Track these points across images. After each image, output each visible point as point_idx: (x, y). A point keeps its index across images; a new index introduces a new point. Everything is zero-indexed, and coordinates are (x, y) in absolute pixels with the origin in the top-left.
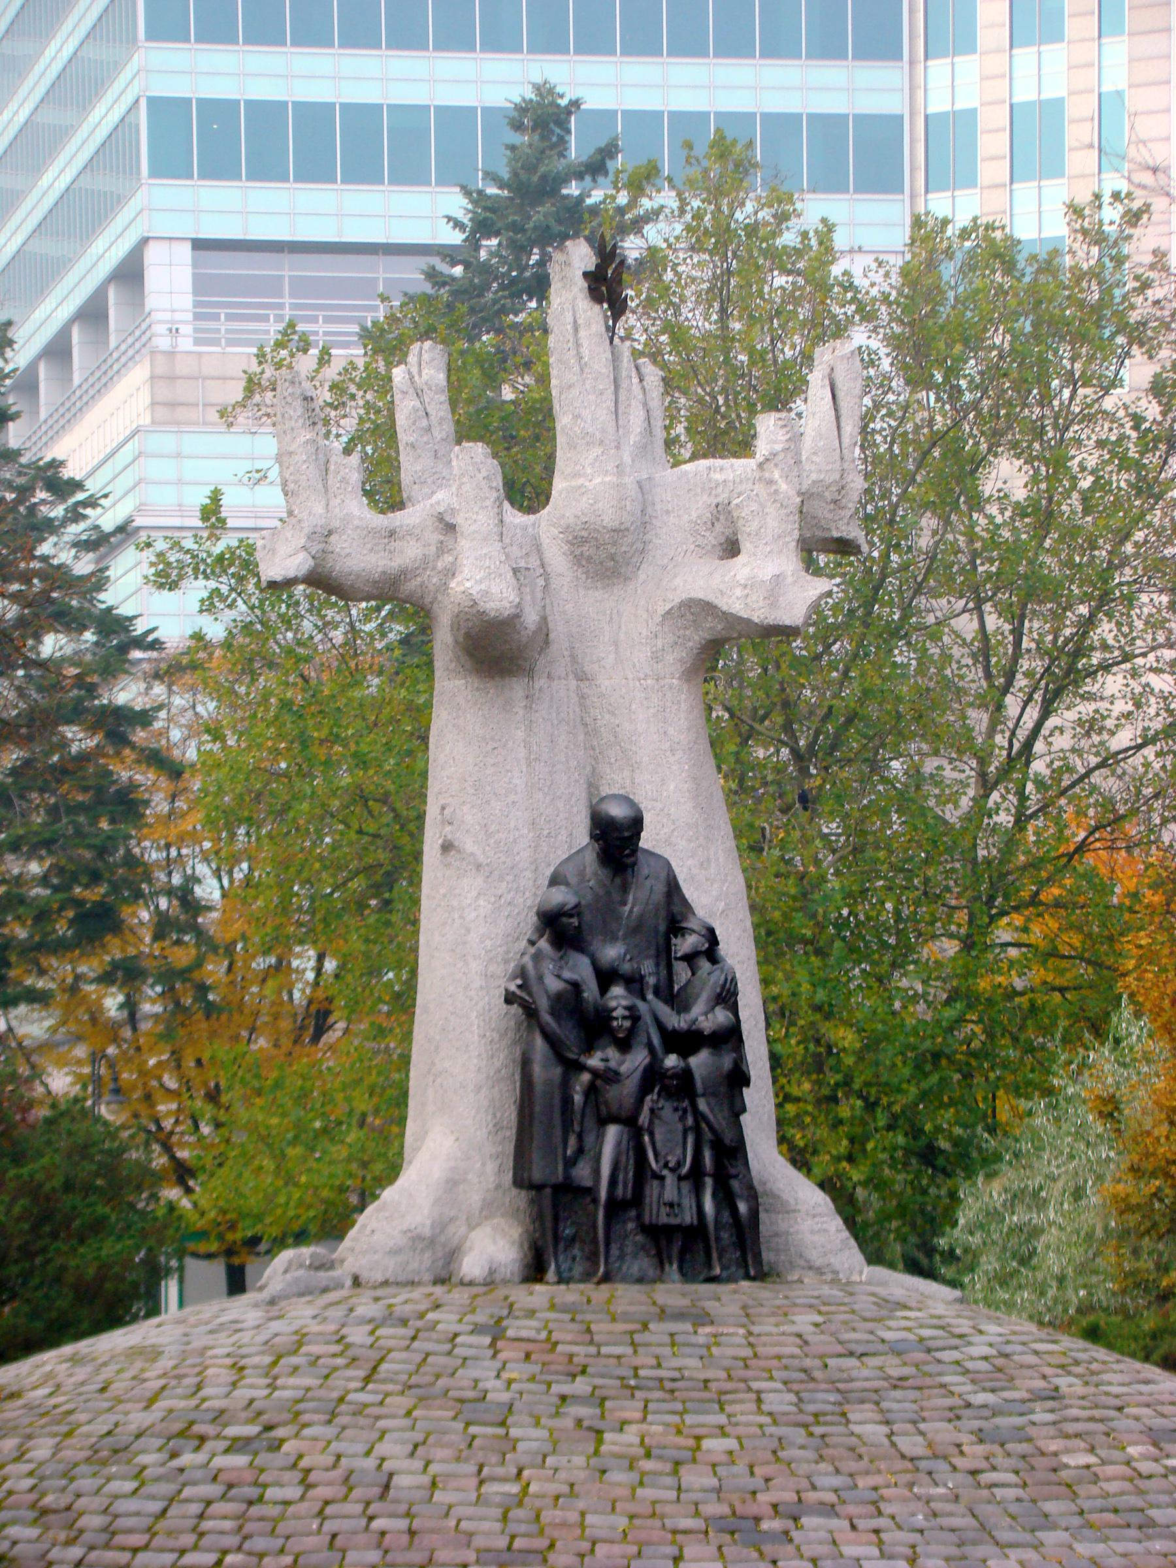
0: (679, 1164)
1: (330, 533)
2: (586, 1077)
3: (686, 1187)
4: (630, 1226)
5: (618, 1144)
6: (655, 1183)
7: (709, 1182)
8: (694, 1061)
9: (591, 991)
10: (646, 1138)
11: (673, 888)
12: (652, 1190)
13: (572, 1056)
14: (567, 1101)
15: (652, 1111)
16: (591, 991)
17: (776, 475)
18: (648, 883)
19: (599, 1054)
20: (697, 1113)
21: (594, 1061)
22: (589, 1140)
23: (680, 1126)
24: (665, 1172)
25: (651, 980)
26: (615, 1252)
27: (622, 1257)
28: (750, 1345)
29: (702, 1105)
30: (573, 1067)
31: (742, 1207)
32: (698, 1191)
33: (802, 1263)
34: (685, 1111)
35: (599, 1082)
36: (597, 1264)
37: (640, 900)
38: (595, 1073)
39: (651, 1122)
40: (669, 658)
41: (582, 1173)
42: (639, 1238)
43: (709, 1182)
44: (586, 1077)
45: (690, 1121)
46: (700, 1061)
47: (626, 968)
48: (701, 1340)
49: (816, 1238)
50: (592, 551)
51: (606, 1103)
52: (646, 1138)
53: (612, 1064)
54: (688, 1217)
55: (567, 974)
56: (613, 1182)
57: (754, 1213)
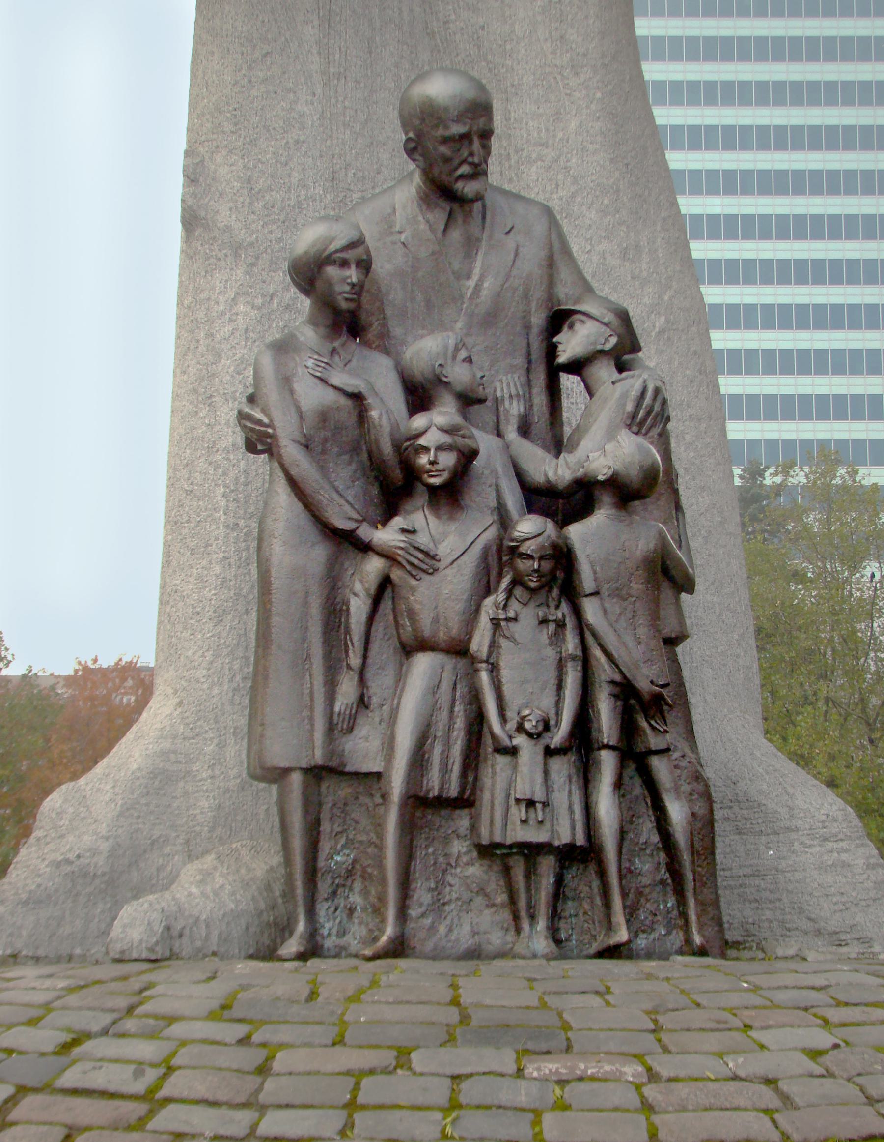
2: (374, 566)
3: (561, 768)
4: (458, 847)
5: (434, 689)
6: (502, 761)
7: (607, 762)
8: (576, 531)
9: (388, 406)
10: (484, 676)
11: (556, 255)
12: (496, 774)
13: (341, 524)
14: (334, 614)
15: (496, 623)
16: (388, 406)
18: (510, 243)
19: (398, 522)
21: (387, 536)
22: (380, 684)
23: (550, 653)
24: (520, 740)
25: (515, 409)
26: (422, 895)
27: (438, 906)
28: (647, 1107)
29: (591, 610)
30: (347, 542)
31: (677, 812)
32: (586, 775)
33: (805, 924)
34: (561, 625)
35: (396, 575)
36: (383, 921)
37: (497, 269)
38: (388, 556)
39: (493, 645)
41: (363, 749)
42: (476, 870)
43: (607, 762)
44: (374, 566)
45: (571, 644)
46: (592, 536)
47: (459, 375)
48: (522, 1094)
49: (829, 879)
51: (412, 614)
52: (484, 676)
53: (422, 540)
54: (565, 830)
55: (339, 378)
56: (419, 760)
57: (705, 827)
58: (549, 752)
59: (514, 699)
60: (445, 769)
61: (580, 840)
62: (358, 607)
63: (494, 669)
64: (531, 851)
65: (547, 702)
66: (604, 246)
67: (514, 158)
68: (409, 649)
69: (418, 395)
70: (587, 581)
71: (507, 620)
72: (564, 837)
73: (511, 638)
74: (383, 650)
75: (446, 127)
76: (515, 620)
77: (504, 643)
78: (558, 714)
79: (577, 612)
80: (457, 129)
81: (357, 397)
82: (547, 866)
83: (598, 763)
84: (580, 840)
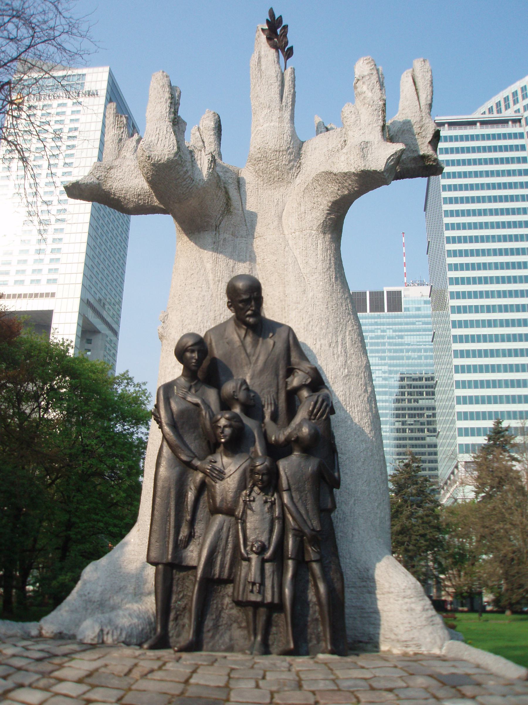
0: (263, 549)
1: (111, 168)
2: (200, 476)
6: (244, 563)
15: (245, 502)
17: (365, 88)
20: (283, 505)
22: (199, 528)
23: (268, 516)
32: (280, 571)
34: (273, 503)
35: (207, 480)
39: (244, 512)
40: (309, 217)
42: (235, 611)
50: (264, 166)
58: (263, 561)
59: (251, 537)
60: (222, 566)
61: (276, 601)
62: (191, 495)
63: (244, 522)
64: (256, 605)
65: (264, 538)
66: (322, 341)
67: (287, 308)
68: (215, 511)
69: (225, 404)
70: (285, 485)
71: (250, 501)
72: (269, 599)
73: (251, 509)
74: (202, 513)
75: (240, 296)
76: (254, 501)
77: (249, 512)
78: (270, 543)
79: (281, 498)
80: (244, 297)
81: (197, 405)
82: (262, 611)
83: (287, 565)
84: (276, 601)
